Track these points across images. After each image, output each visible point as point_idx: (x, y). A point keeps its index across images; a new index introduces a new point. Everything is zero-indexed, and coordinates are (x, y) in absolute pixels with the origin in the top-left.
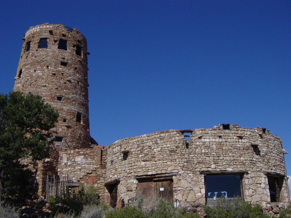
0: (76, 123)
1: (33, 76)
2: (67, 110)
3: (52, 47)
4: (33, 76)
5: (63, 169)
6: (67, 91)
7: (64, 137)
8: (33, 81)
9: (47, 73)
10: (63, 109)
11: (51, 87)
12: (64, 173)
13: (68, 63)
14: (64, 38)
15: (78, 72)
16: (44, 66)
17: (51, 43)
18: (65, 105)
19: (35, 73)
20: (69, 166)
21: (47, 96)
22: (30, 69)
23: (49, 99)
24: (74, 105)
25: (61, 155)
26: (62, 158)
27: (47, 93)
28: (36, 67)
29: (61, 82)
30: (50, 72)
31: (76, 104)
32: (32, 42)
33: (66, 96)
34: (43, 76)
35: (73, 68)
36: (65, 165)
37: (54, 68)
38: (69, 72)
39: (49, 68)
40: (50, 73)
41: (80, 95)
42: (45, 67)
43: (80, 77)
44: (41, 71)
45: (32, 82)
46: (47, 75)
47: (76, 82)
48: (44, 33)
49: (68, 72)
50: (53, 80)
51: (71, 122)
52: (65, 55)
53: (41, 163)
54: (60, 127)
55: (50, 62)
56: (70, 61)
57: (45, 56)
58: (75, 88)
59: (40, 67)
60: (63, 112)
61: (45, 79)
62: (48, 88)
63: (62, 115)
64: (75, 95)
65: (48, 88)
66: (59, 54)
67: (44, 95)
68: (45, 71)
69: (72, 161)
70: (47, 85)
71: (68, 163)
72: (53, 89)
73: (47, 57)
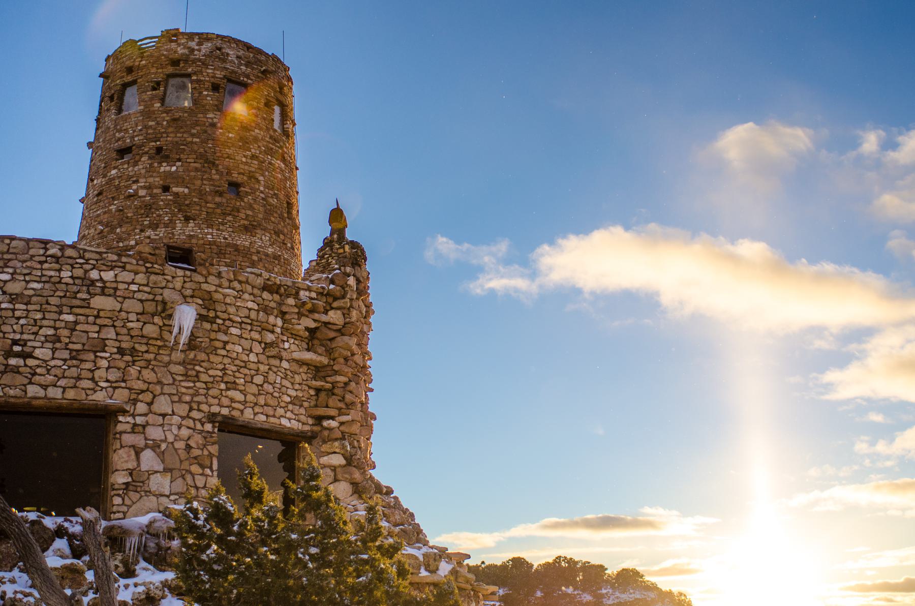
6: (124, 230)
13: (134, 145)
15: (166, 158)
33: (121, 244)
35: (146, 153)
47: (155, 191)
64: (149, 232)
70: (86, 233)
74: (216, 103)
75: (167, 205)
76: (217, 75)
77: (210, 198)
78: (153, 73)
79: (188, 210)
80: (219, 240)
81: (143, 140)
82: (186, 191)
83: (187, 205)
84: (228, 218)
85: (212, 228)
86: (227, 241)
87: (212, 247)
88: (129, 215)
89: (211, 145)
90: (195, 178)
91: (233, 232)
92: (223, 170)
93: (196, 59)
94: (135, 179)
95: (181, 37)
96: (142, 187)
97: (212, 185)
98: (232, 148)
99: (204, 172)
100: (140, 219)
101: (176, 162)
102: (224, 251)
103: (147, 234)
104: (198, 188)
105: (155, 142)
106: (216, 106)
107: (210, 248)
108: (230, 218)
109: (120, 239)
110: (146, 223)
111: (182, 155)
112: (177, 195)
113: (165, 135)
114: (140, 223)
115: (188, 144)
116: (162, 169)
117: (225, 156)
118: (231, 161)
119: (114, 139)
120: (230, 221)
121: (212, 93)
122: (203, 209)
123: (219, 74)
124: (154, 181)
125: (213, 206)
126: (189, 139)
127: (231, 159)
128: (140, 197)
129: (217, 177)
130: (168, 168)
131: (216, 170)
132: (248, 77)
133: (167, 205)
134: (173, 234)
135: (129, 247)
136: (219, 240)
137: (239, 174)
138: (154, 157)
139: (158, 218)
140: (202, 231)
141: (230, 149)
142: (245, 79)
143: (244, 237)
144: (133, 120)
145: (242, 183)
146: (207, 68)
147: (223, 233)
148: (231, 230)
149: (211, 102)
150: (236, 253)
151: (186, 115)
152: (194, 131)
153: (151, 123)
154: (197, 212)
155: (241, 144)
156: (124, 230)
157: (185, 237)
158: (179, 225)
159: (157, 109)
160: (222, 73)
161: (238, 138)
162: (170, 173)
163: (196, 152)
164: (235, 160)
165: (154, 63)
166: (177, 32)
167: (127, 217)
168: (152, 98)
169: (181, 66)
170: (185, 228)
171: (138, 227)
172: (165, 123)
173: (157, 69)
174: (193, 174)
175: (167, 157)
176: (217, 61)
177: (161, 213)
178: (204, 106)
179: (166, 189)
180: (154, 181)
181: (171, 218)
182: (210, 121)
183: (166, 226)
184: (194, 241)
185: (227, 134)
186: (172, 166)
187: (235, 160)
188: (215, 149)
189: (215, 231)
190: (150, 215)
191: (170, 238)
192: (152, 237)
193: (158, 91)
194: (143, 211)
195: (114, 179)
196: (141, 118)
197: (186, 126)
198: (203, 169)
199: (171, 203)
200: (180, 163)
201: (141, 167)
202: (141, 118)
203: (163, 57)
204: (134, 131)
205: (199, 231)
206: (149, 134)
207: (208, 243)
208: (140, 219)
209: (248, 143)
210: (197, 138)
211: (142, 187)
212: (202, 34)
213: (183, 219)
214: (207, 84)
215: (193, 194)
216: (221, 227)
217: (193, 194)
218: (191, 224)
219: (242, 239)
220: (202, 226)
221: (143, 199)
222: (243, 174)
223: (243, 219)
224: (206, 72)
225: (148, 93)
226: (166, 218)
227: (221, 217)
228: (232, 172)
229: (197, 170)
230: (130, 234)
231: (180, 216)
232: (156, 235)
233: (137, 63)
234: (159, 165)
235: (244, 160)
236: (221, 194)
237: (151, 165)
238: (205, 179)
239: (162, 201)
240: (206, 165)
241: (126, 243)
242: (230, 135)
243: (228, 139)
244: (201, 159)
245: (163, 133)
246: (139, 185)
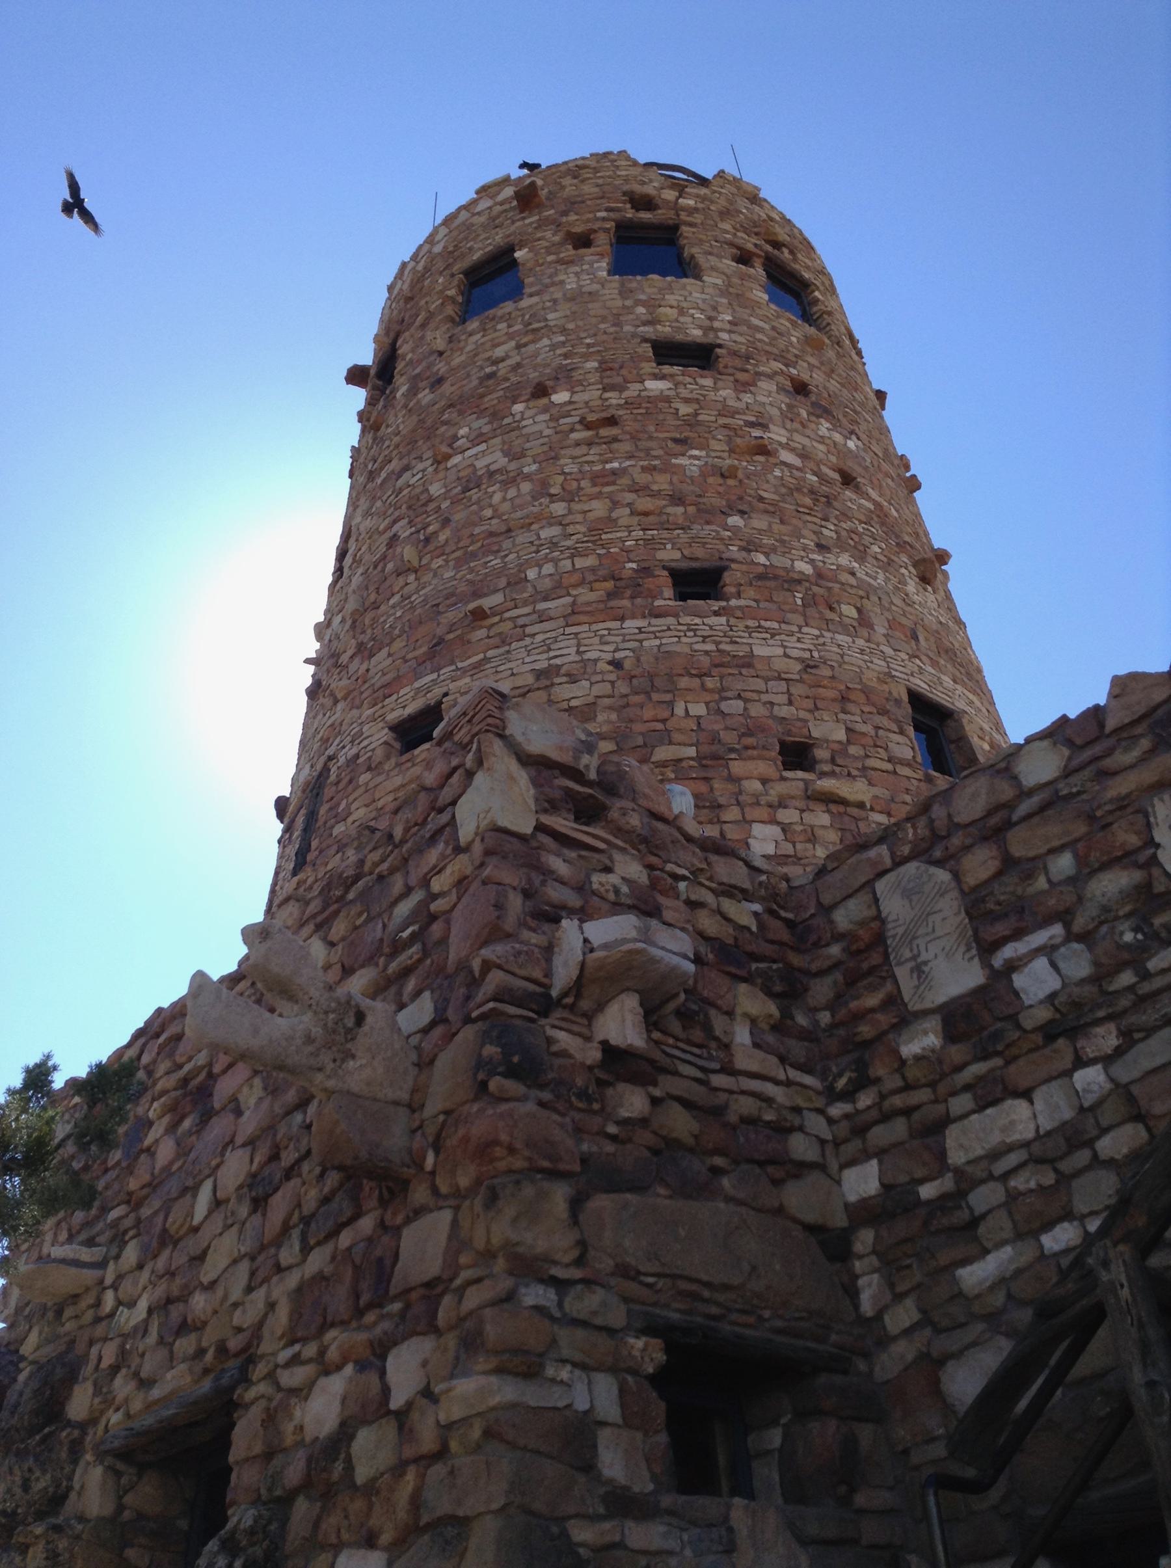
1: (430, 500)
2: (798, 667)
3: (562, 277)
4: (430, 500)
5: (953, 1135)
8: (431, 529)
9: (547, 432)
10: (751, 654)
11: (591, 516)
12: (984, 1197)
13: (720, 346)
14: (645, 216)
15: (822, 411)
16: (514, 403)
17: (550, 258)
18: (768, 624)
19: (441, 475)
20: (1050, 1033)
21: (576, 577)
22: (407, 468)
23: (588, 604)
24: (864, 632)
25: (843, 918)
26: (879, 939)
27: (566, 565)
28: (450, 433)
29: (680, 466)
30: (562, 421)
31: (880, 630)
32: (411, 325)
34: (513, 466)
36: (957, 1053)
37: (605, 390)
38: (741, 405)
39: (561, 397)
40: (572, 430)
41: (888, 565)
42: (518, 408)
43: (851, 444)
44: (498, 440)
45: (427, 540)
46: (545, 448)
48: (481, 237)
49: (731, 403)
50: (616, 465)
51: (871, 763)
52: (685, 305)
53: (468, 1033)
54: (762, 813)
55: (558, 361)
56: (735, 337)
57: (513, 343)
59: (486, 420)
60: (760, 684)
61: (528, 477)
62: (570, 530)
63: (757, 710)
64: (844, 560)
65: (570, 530)
66: (628, 303)
67: (547, 583)
68: (524, 431)
69: (1080, 923)
71: (1018, 980)
72: (621, 522)
73: (525, 345)
78: (727, 232)
94: (753, 419)
130: (837, 437)
167: (761, 499)
171: (805, 532)
192: (858, 575)
202: (724, 301)
237: (789, 406)
241: (778, 561)
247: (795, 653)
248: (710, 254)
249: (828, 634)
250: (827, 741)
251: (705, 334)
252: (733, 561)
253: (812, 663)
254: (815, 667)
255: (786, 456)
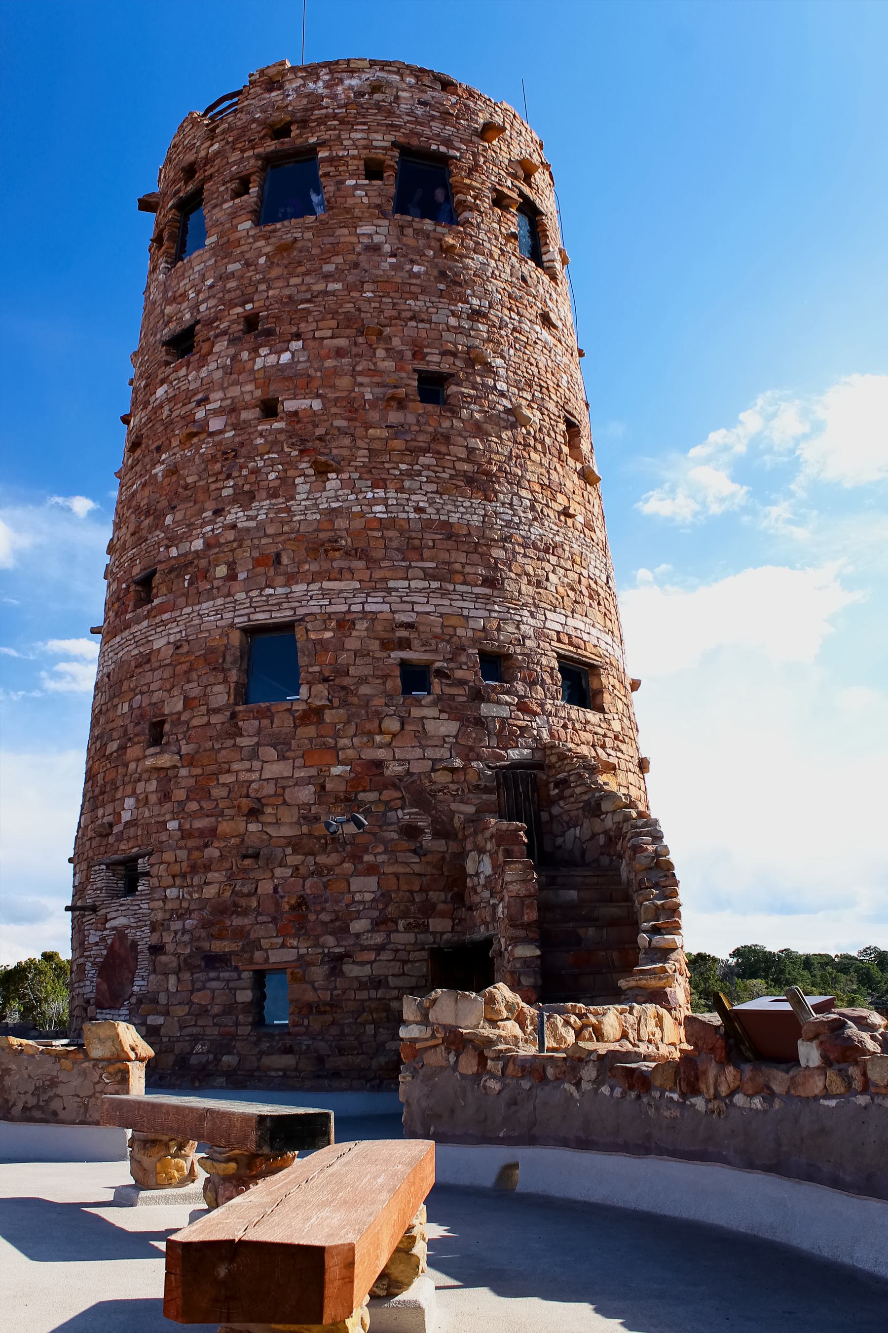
0: (234, 716)
7: (143, 857)
13: (197, 322)
31: (242, 576)
33: (174, 552)
35: (225, 333)
47: (245, 415)
58: (235, 456)
64: (235, 515)
74: (378, 201)
75: (274, 444)
76: (375, 143)
77: (374, 416)
78: (235, 163)
79: (322, 450)
80: (404, 515)
81: (216, 306)
82: (317, 405)
83: (320, 439)
84: (422, 460)
85: (385, 488)
86: (424, 516)
87: (390, 534)
88: (190, 480)
89: (369, 294)
90: (336, 372)
91: (437, 492)
92: (404, 348)
93: (327, 116)
94: (200, 396)
95: (290, 76)
96: (217, 412)
97: (378, 384)
98: (421, 297)
99: (357, 355)
100: (213, 486)
101: (289, 341)
102: (417, 542)
103: (230, 518)
104: (344, 394)
105: (243, 305)
106: (378, 206)
107: (382, 537)
108: (427, 459)
109: (173, 540)
110: (226, 493)
111: (303, 325)
112: (294, 414)
113: (263, 287)
114: (214, 495)
115: (317, 297)
116: (259, 363)
117: (409, 314)
118: (421, 325)
119: (161, 322)
120: (428, 467)
121: (367, 182)
122: (360, 443)
123: (381, 140)
124: (242, 393)
125: (385, 433)
126: (320, 287)
127: (422, 321)
128: (212, 434)
129: (390, 365)
130: (272, 359)
131: (387, 350)
132: (448, 143)
133: (274, 444)
134: (288, 510)
135: (190, 557)
136: (404, 515)
137: (444, 353)
138: (239, 339)
139: (253, 478)
140: (360, 496)
141: (416, 299)
142: (443, 149)
143: (467, 504)
144: (197, 269)
145: (452, 375)
146: (352, 130)
147: (413, 497)
148: (432, 487)
149: (365, 200)
150: (450, 544)
151: (309, 235)
152: (329, 268)
153: (231, 268)
154: (345, 452)
155: (442, 286)
156: (179, 516)
157: (318, 517)
158: (302, 488)
159: (245, 233)
160: (387, 137)
161: (435, 273)
162: (279, 367)
163: (334, 314)
164: (431, 322)
165: (234, 142)
166: (281, 68)
167: (186, 488)
168: (233, 215)
169: (292, 134)
170: (318, 495)
171: (207, 505)
172: (262, 260)
173: (243, 151)
174: (329, 363)
175: (269, 333)
176: (375, 114)
177: (261, 464)
178: (348, 211)
179: (269, 409)
180: (242, 393)
181: (282, 475)
182: (365, 240)
183: (273, 494)
184: (341, 523)
185: (408, 267)
186: (279, 353)
187: (431, 322)
188: (380, 302)
189: (392, 494)
190: (235, 474)
191: (283, 523)
192: (239, 525)
193: (246, 197)
194: (218, 466)
195: (161, 406)
196: (213, 260)
197: (311, 258)
198: (355, 350)
199: (282, 437)
200: (300, 343)
201: (213, 366)
203: (254, 126)
204: (198, 293)
205: (352, 497)
206: (229, 291)
207: (375, 525)
208: (213, 486)
209: (460, 285)
210: (336, 281)
211: (217, 412)
212: (337, 63)
213: (311, 472)
214: (356, 162)
215: (334, 410)
216: (407, 484)
217: (334, 410)
218: (333, 482)
219: (462, 509)
220: (359, 484)
221: (217, 438)
222: (454, 354)
223: (460, 459)
224: (350, 138)
225: (225, 206)
226: (272, 476)
227: (408, 459)
228: (425, 350)
229: (339, 353)
230: (192, 524)
231: (304, 465)
232: (250, 518)
233: (203, 154)
234: (253, 355)
235: (453, 321)
236: (401, 404)
237: (234, 358)
238: (361, 373)
239: (261, 435)
240: (360, 340)
241: (184, 547)
242: (416, 269)
243: (410, 277)
244: (348, 327)
245: (260, 282)
246: (208, 407)
247: (172, 639)
248: (215, 206)
249: (197, 608)
250: (172, 714)
251: (192, 314)
252: (160, 562)
253: (179, 644)
254: (181, 646)
255: (215, 424)
